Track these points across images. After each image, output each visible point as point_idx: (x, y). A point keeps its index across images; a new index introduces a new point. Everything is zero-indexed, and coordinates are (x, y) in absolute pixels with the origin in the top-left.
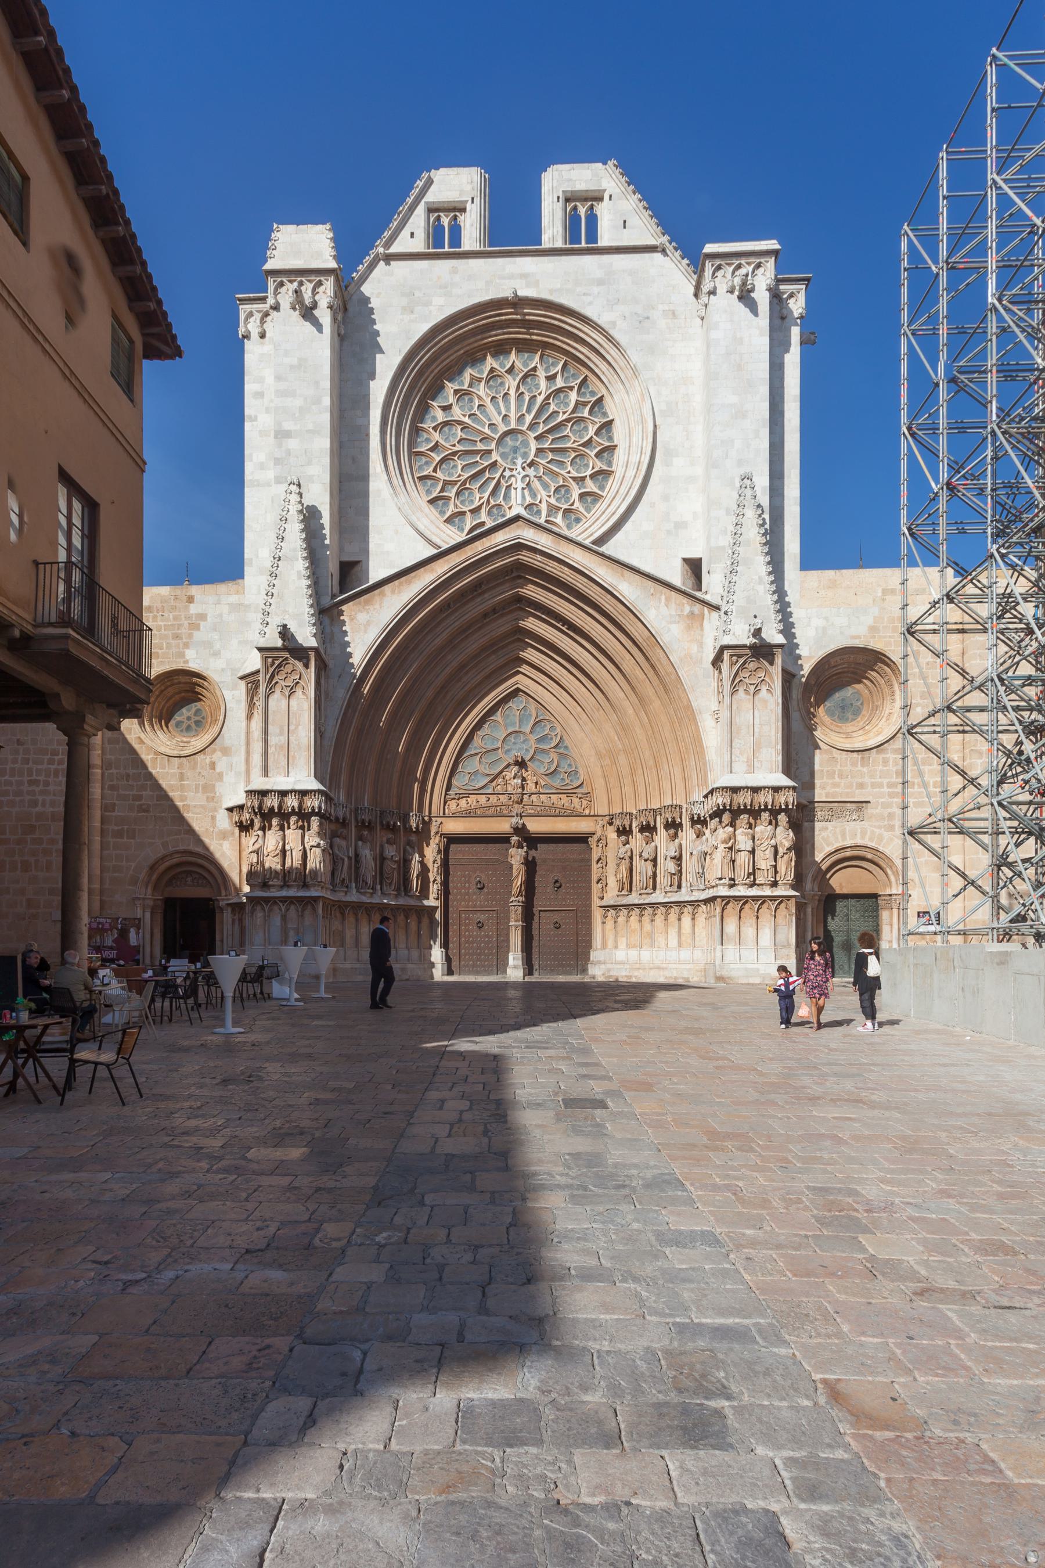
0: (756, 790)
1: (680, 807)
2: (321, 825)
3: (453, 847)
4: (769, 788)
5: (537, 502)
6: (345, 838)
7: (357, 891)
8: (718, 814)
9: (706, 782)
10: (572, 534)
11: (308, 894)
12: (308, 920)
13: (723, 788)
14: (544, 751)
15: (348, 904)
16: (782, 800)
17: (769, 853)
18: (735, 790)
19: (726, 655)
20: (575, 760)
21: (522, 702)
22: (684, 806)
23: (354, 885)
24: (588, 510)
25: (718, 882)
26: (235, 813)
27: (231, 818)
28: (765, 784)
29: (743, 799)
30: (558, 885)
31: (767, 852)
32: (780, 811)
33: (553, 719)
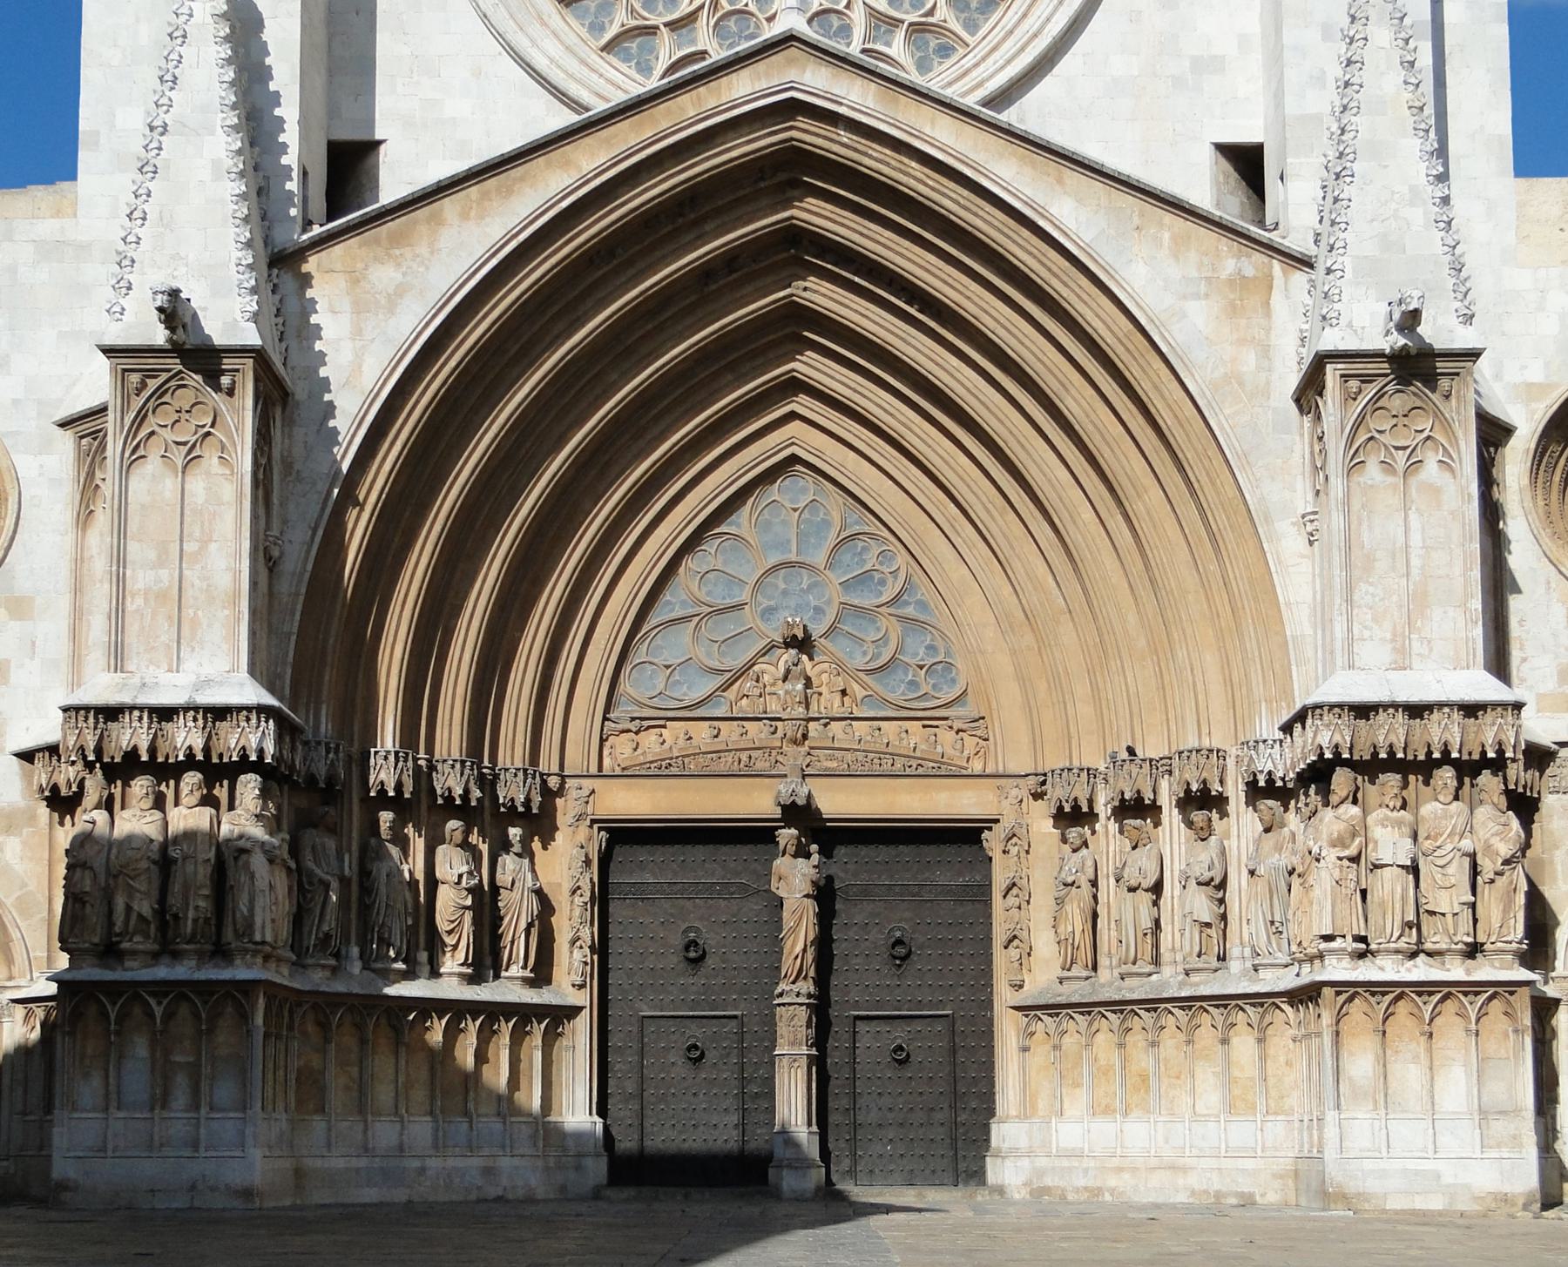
0: (1416, 711)
1: (1221, 754)
2: (265, 794)
3: (620, 853)
4: (1450, 705)
5: (841, 7)
6: (333, 830)
7: (366, 967)
8: (1318, 774)
9: (1287, 693)
10: (933, 83)
11: (226, 974)
12: (224, 1039)
13: (1332, 707)
14: (860, 611)
15: (336, 1000)
16: (1489, 738)
17: (1458, 872)
18: (1363, 711)
19: (1332, 373)
20: (943, 636)
21: (804, 490)
22: (1233, 751)
23: (355, 951)
24: (972, 27)
25: (1324, 946)
26: (38, 764)
27: (27, 778)
28: (1443, 698)
29: (1389, 733)
30: (901, 951)
31: (1451, 870)
32: (1483, 763)
33: (886, 534)
